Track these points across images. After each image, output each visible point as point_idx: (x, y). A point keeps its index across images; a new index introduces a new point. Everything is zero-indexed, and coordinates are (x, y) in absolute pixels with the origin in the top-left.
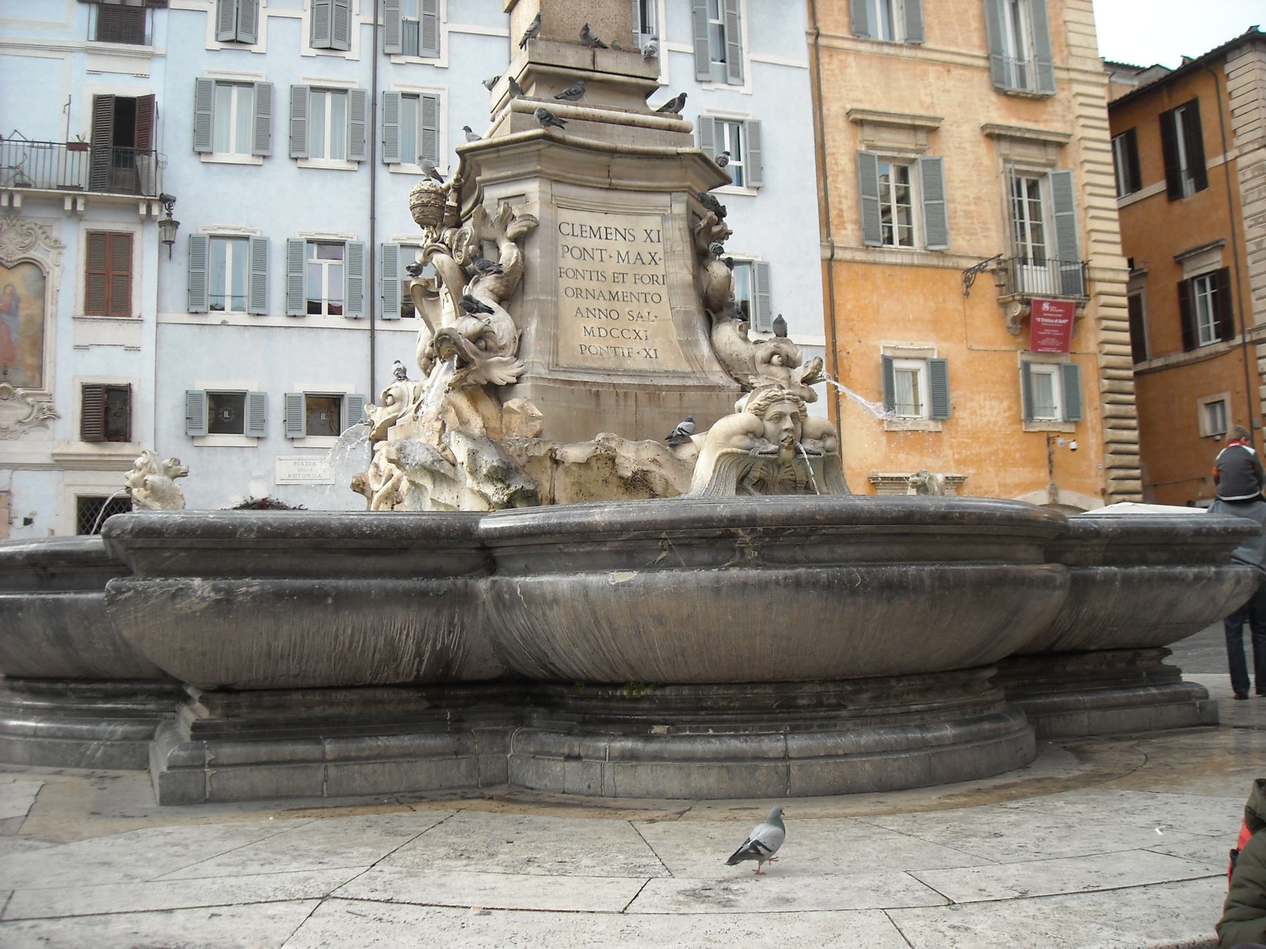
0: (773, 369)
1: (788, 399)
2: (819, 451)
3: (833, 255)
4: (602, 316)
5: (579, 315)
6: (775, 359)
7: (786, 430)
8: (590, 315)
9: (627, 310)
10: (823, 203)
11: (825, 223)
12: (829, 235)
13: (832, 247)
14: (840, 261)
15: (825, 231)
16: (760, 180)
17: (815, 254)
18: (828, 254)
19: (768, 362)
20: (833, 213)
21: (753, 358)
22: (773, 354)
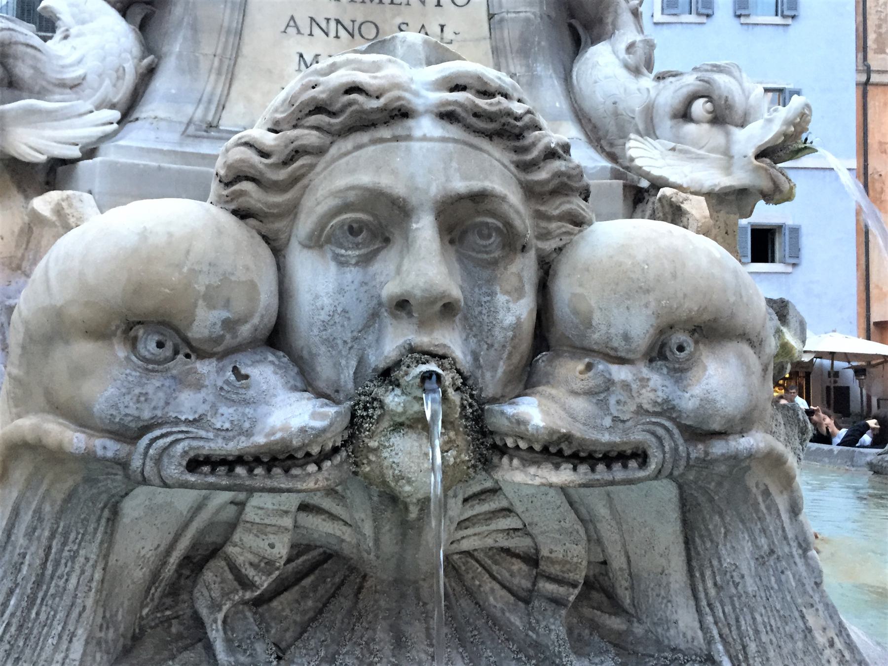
0: (690, 128)
1: (448, 116)
2: (638, 436)
3: (868, 79)
4: (342, 33)
5: (292, 31)
6: (699, 107)
7: (402, 305)
8: (317, 31)
9: (399, 20)
10: (861, 29)
11: (863, 48)
12: (865, 58)
13: (868, 71)
14: (877, 85)
15: (861, 56)
16: (796, 9)
17: (851, 77)
18: (863, 78)
19: (684, 115)
20: (871, 36)
21: (649, 112)
22: (693, 97)
